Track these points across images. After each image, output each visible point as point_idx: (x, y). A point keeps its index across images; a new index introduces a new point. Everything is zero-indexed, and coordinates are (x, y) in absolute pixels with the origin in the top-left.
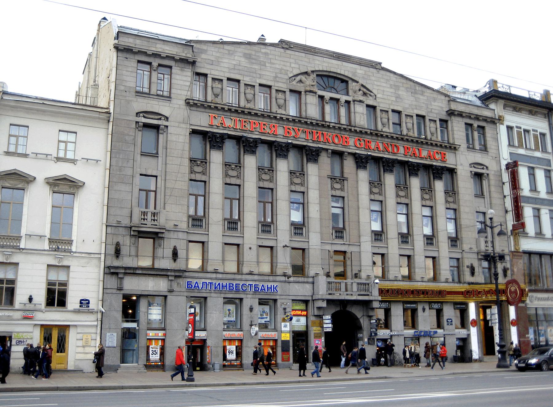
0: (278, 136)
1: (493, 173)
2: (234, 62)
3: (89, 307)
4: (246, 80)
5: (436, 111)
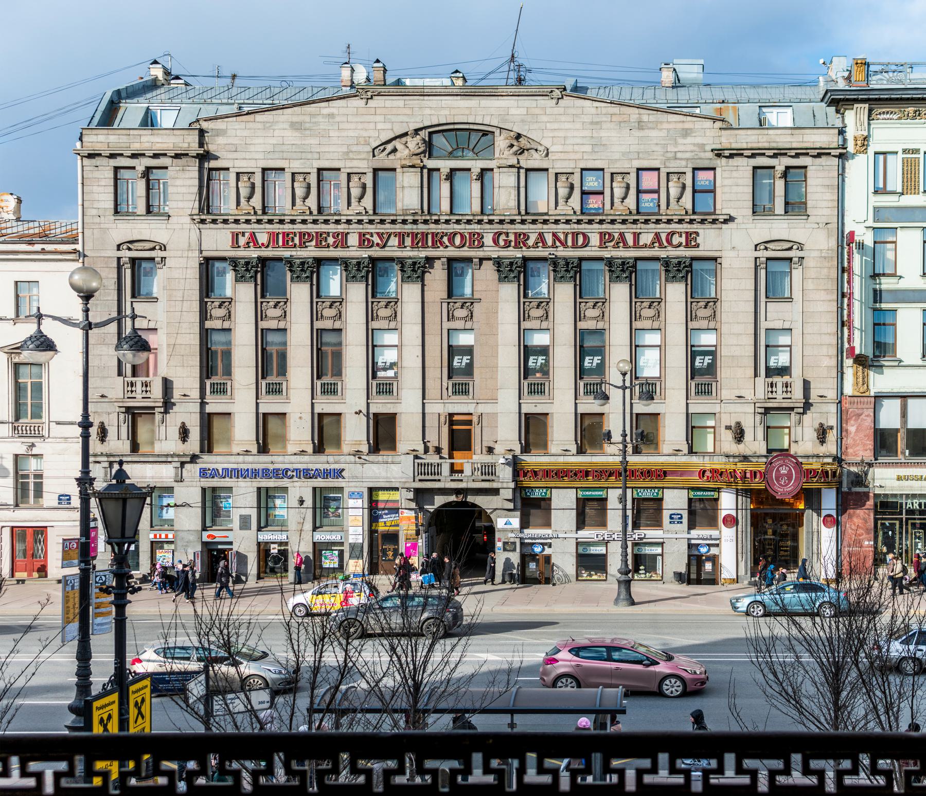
0: (351, 249)
1: (815, 254)
2: (274, 141)
4: (296, 166)
5: (688, 155)
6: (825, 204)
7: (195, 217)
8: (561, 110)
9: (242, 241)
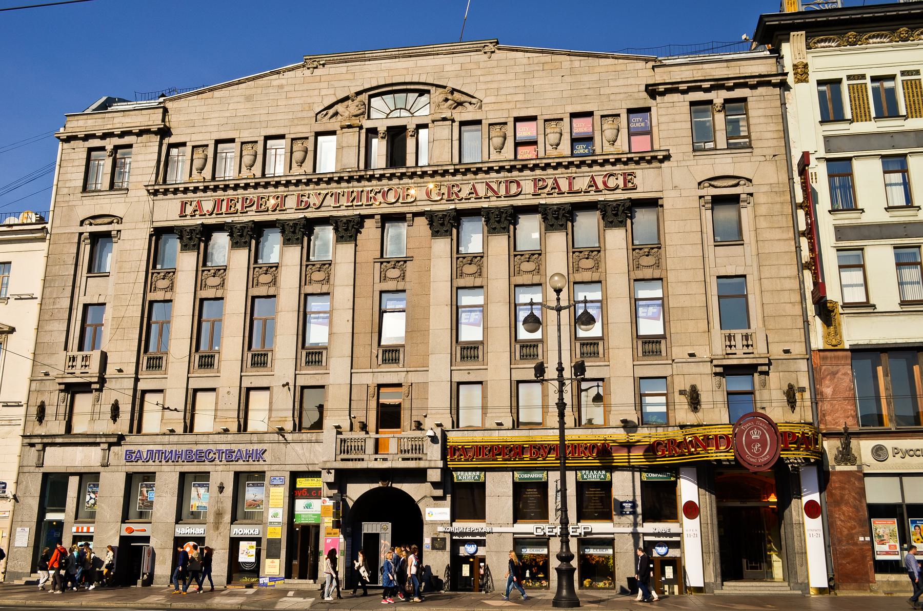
0: (288, 211)
1: (765, 189)
2: (227, 114)
3: (4, 492)
4: (246, 136)
6: (769, 135)
7: (149, 188)
8: (494, 63)
9: (189, 210)
